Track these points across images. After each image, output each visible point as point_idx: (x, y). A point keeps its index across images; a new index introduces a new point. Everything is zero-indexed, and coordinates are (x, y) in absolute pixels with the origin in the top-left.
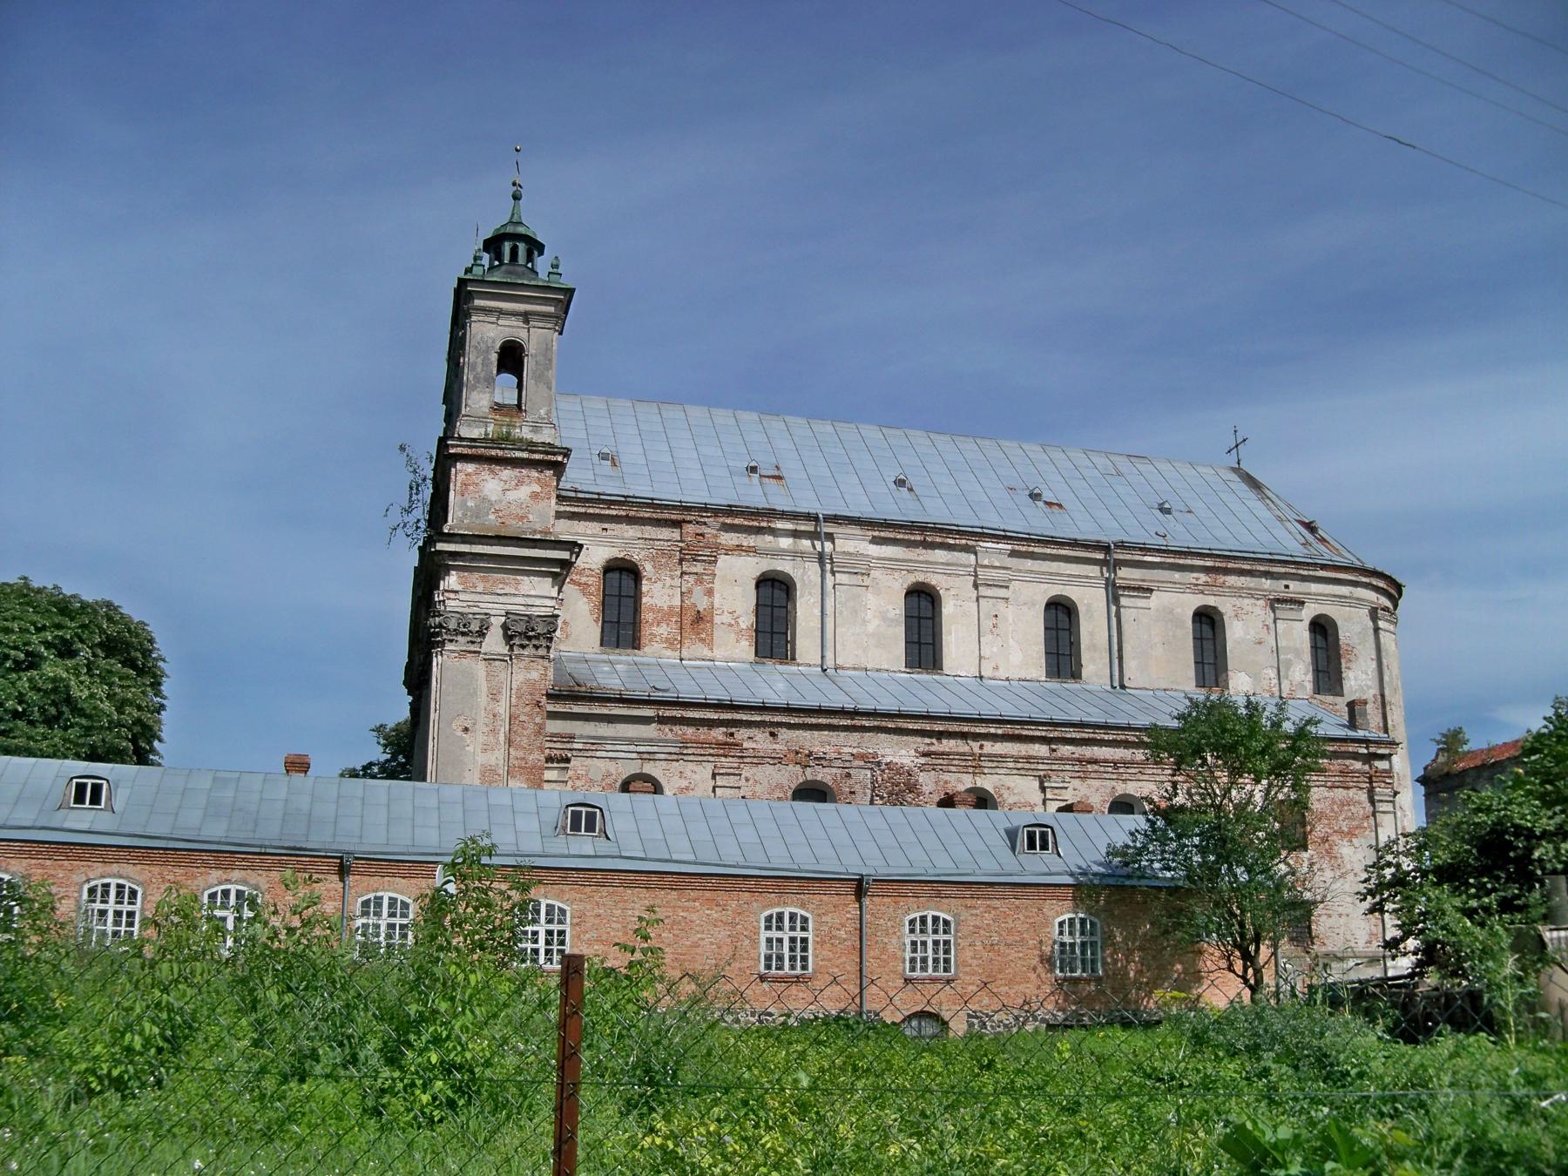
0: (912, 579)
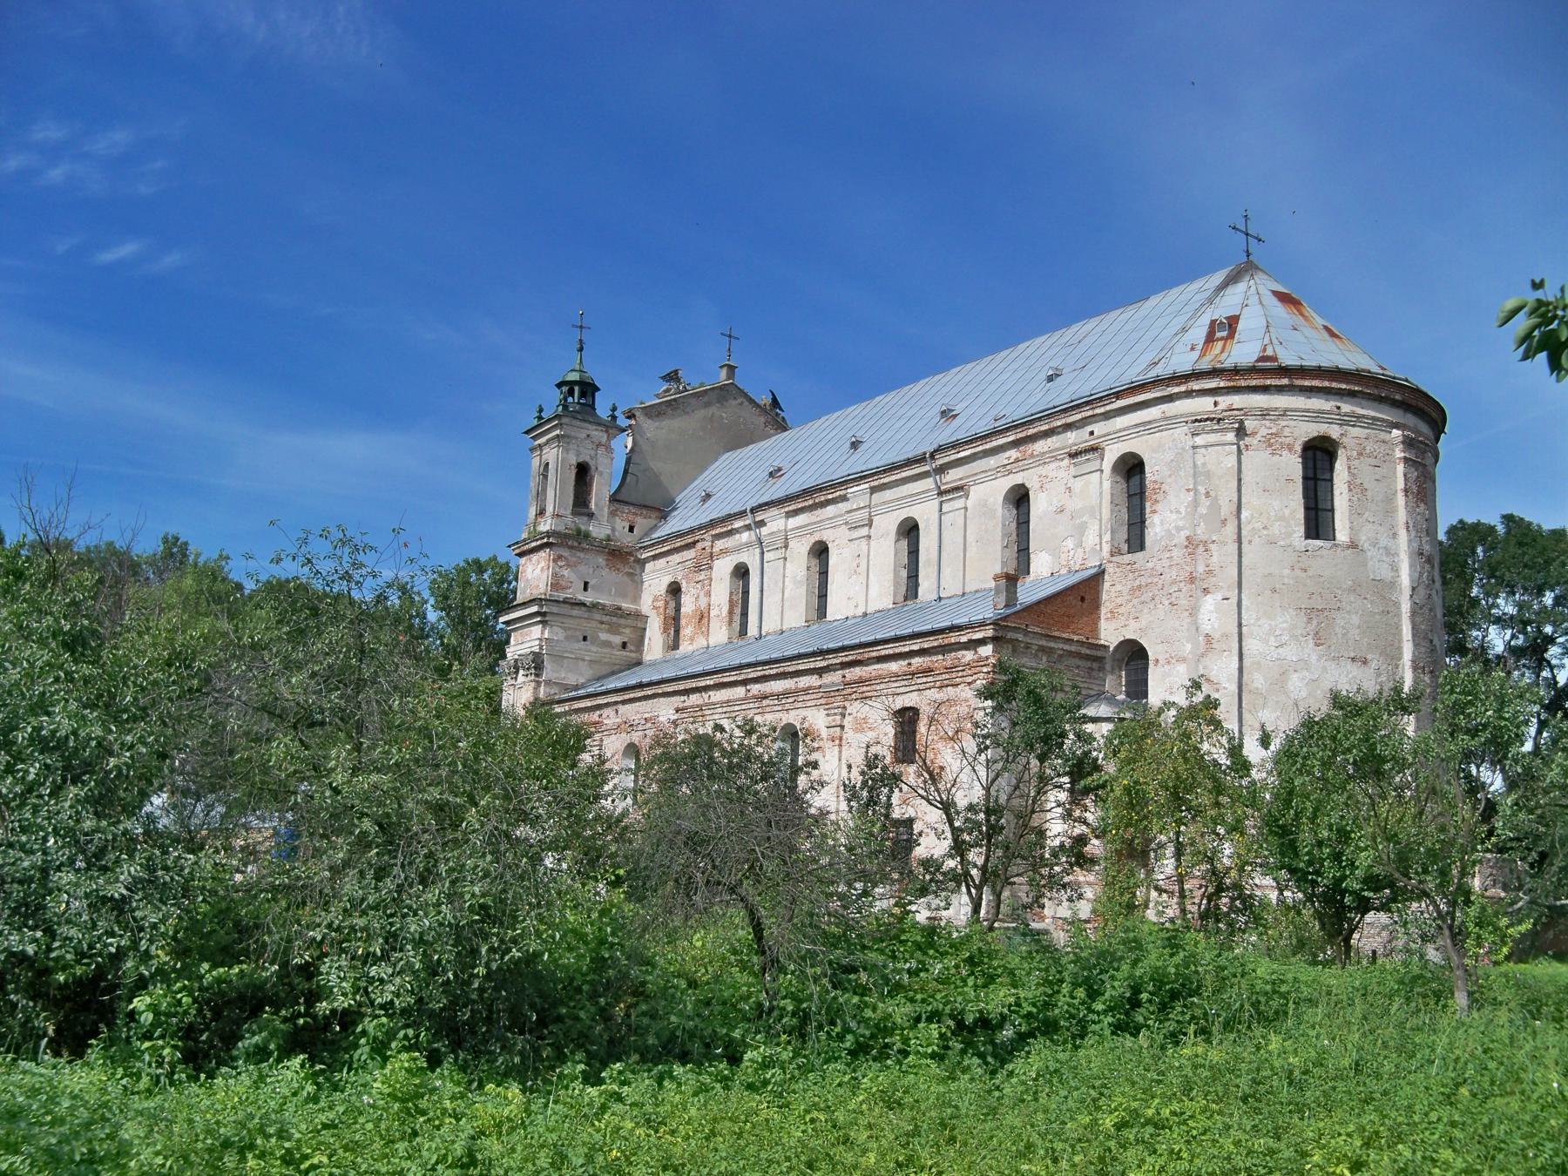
0: (813, 540)
